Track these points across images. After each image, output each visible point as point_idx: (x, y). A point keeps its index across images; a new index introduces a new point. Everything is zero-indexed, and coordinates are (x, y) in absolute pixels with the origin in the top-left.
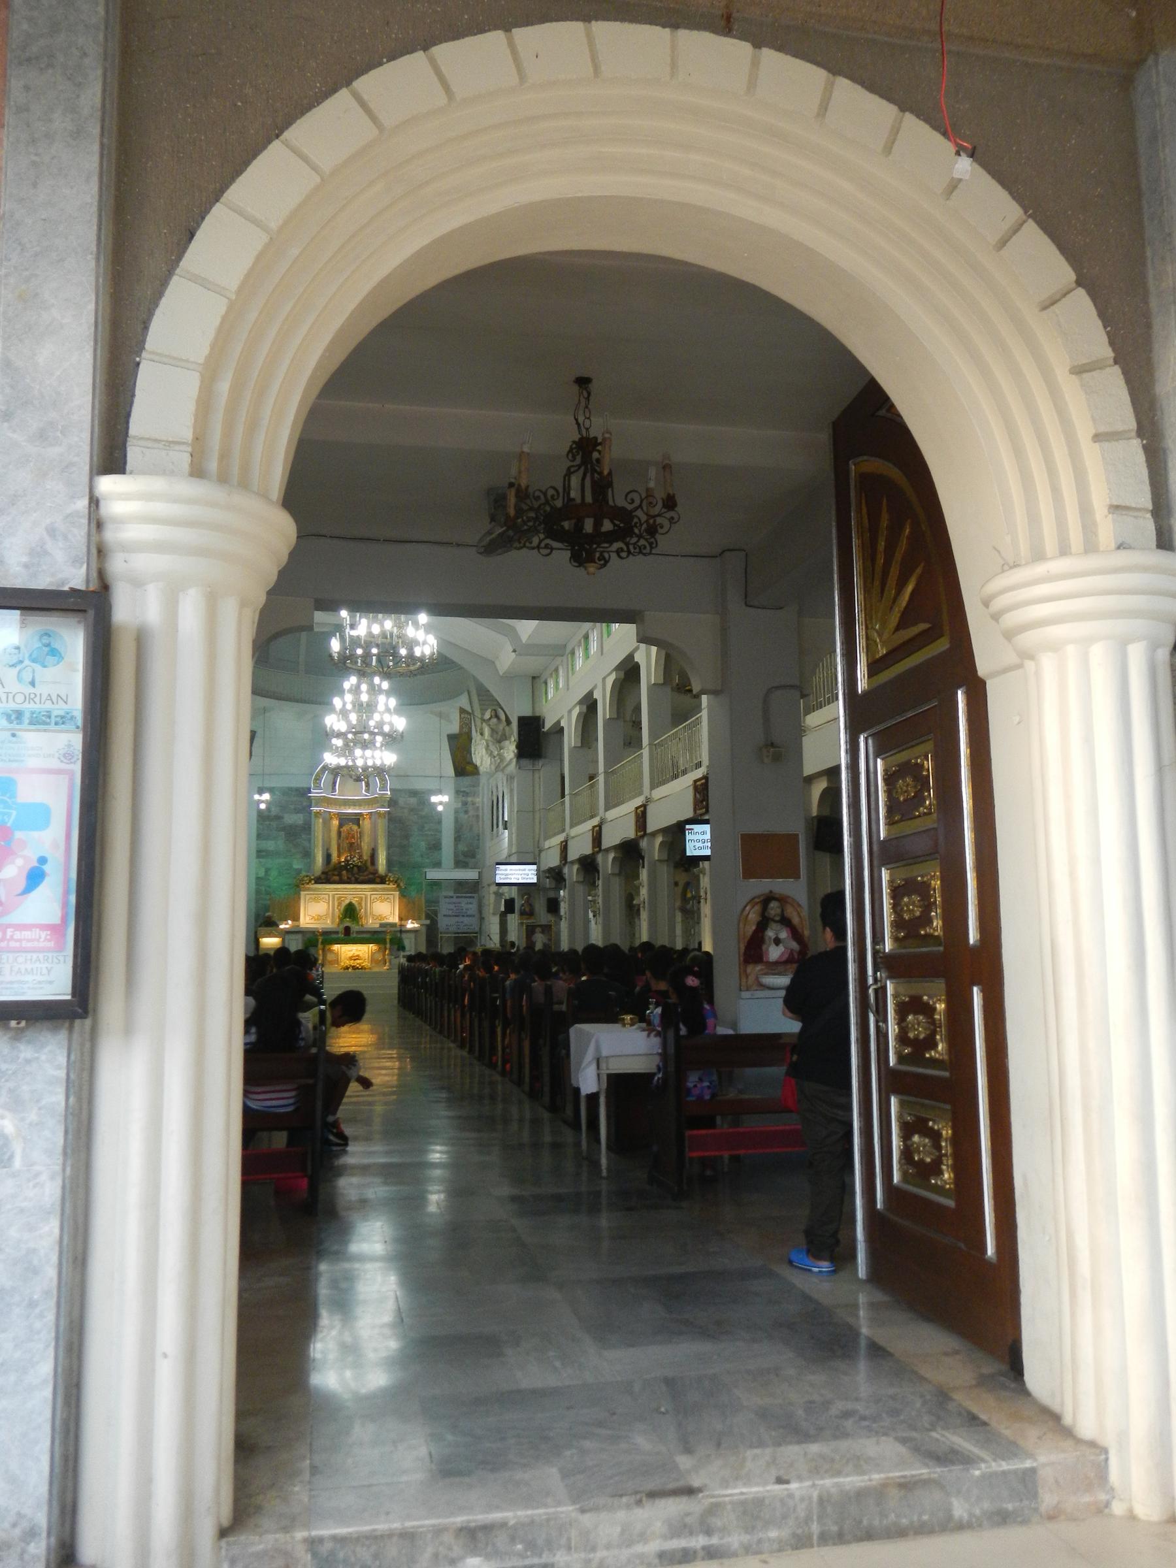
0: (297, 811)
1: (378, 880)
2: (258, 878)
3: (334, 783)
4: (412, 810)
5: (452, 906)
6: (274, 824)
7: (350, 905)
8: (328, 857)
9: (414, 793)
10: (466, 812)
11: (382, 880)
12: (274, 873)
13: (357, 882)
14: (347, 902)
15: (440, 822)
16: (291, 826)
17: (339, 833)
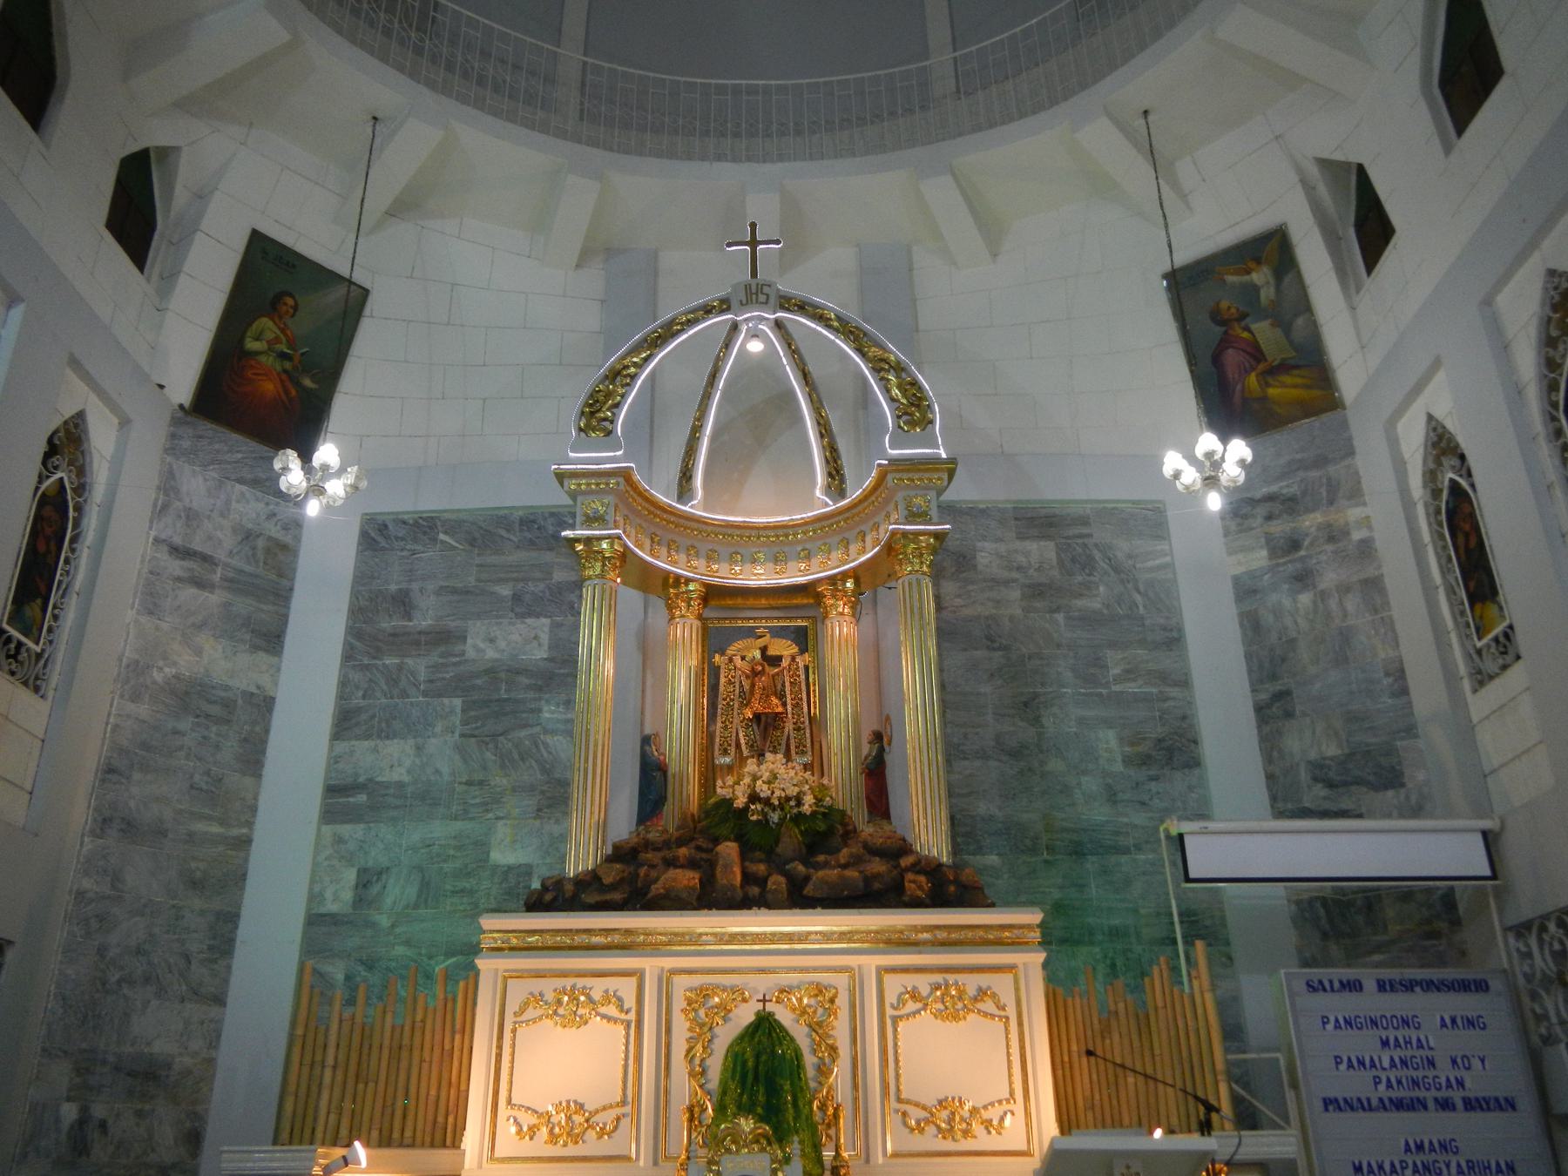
0: (522, 606)
1: (916, 884)
2: (315, 920)
3: (686, 476)
4: (1036, 591)
5: (1364, 1043)
6: (419, 665)
7: (764, 1026)
8: (653, 779)
9: (1039, 522)
10: (1303, 579)
11: (947, 888)
12: (397, 892)
13: (799, 898)
14: (745, 1015)
15: (1173, 640)
16: (491, 672)
17: (709, 678)
